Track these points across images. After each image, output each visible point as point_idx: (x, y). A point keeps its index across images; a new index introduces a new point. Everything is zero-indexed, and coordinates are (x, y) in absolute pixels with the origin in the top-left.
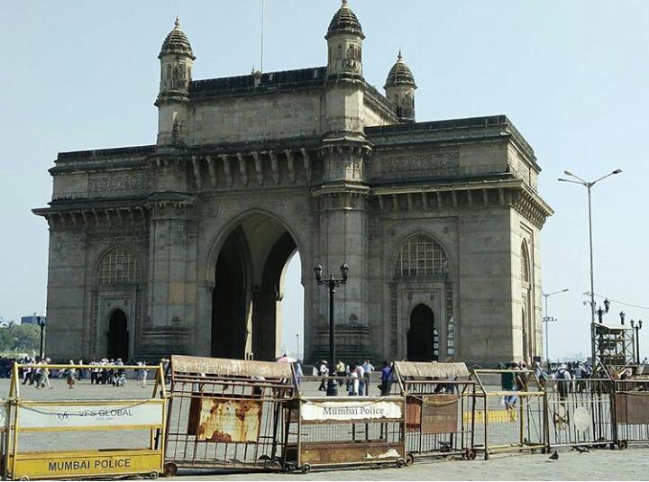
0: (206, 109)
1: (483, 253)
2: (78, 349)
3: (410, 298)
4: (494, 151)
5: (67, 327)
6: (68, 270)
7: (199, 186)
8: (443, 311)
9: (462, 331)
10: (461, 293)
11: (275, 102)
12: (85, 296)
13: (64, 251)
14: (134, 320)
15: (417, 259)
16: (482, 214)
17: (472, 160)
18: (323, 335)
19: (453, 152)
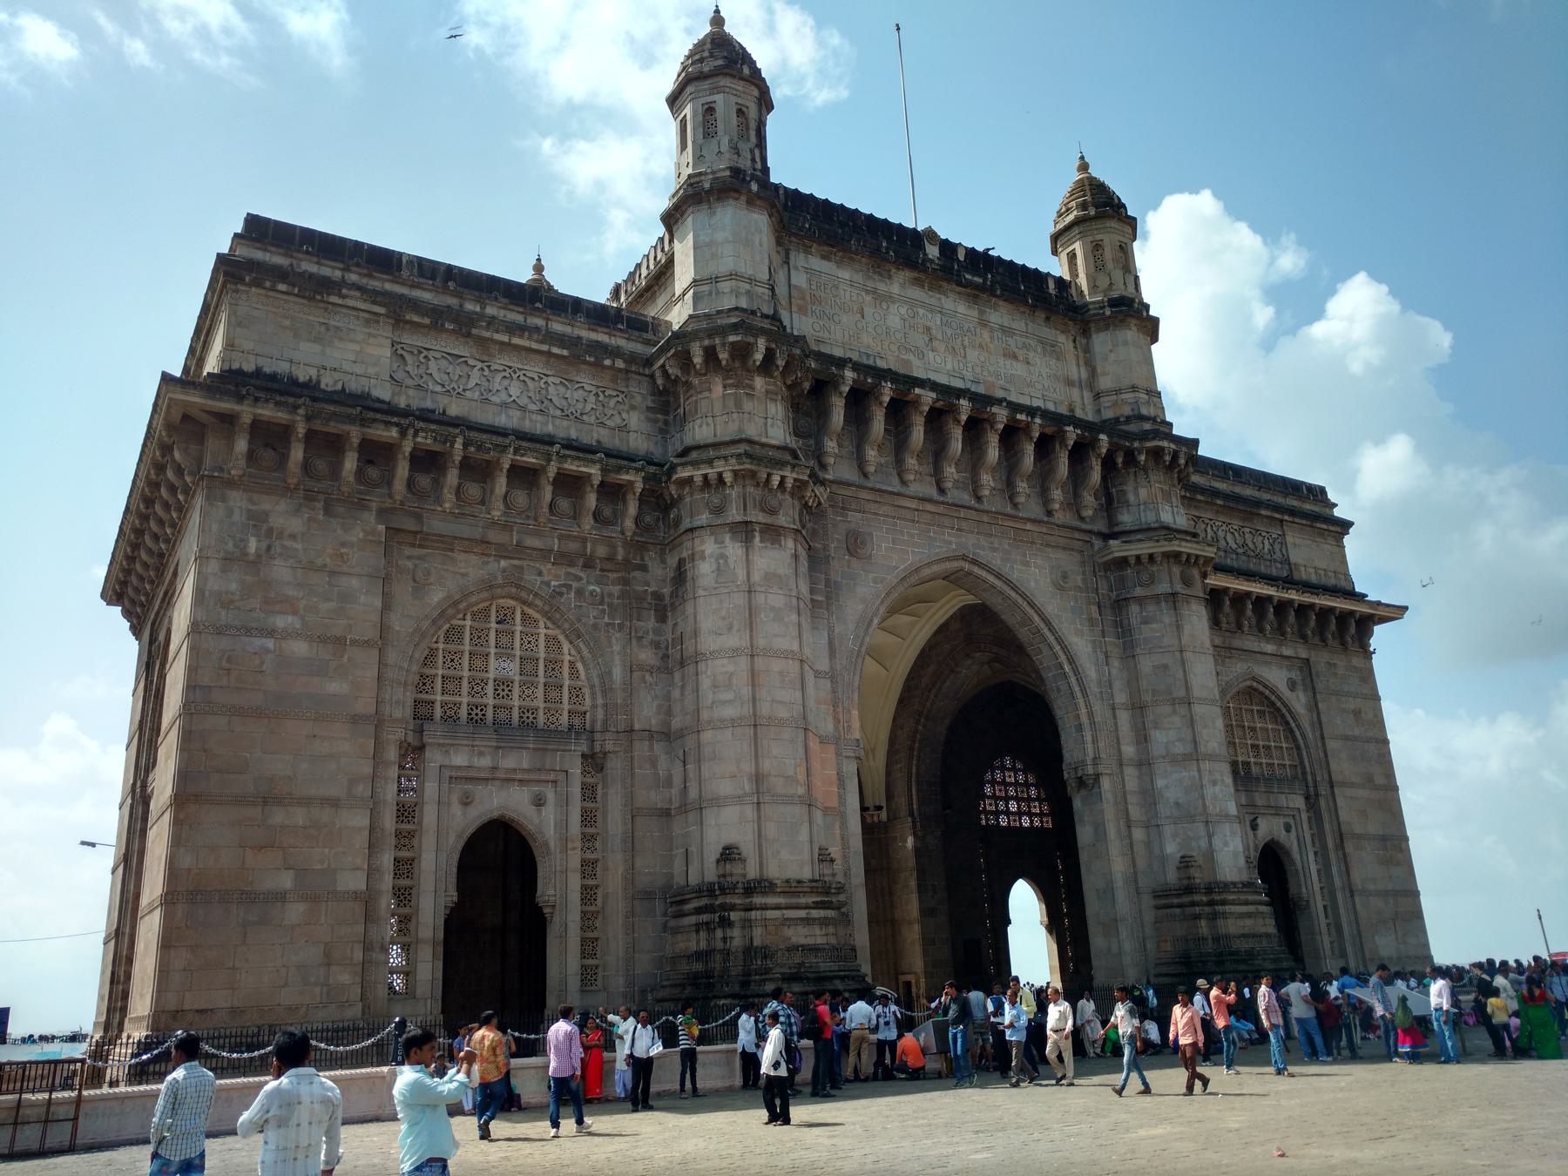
0: (816, 263)
1: (1355, 739)
2: (344, 977)
3: (1254, 827)
4: (1328, 547)
5: (286, 881)
6: (300, 648)
7: (831, 460)
8: (1311, 856)
9: (1357, 899)
10: (1341, 819)
11: (982, 313)
12: (377, 758)
13: (281, 571)
14: (575, 861)
15: (1249, 742)
16: (1340, 661)
17: (1303, 552)
18: (1219, 908)
19: (1275, 532)
